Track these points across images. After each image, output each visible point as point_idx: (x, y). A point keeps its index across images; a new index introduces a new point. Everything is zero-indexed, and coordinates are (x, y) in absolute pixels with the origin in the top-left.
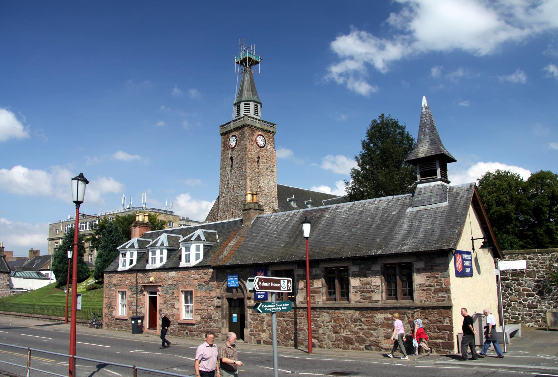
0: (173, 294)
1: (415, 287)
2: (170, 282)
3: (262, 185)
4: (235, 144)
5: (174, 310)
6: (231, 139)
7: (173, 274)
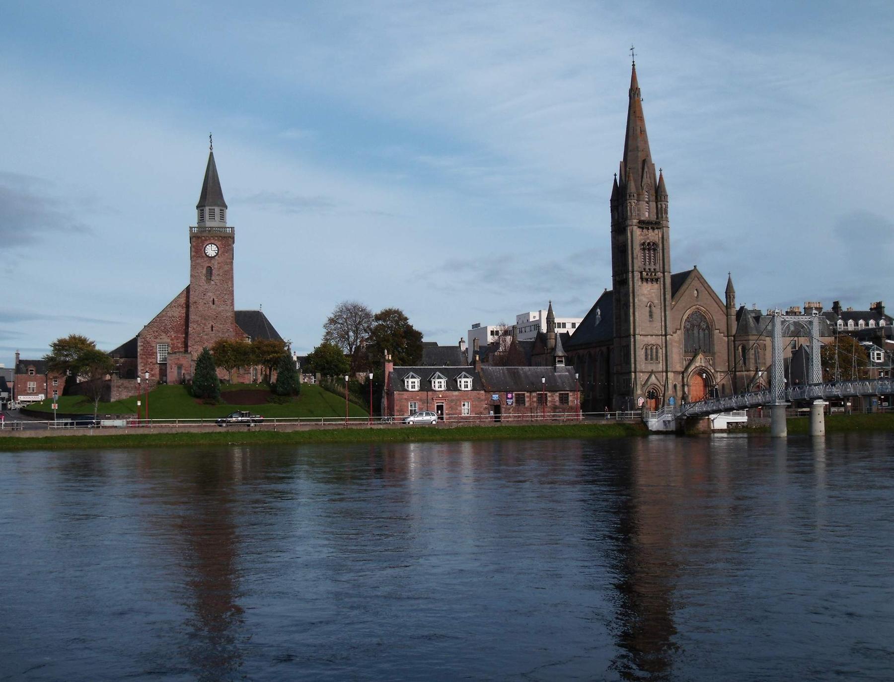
0: (456, 403)
1: (569, 401)
2: (454, 398)
4: (215, 254)
6: (208, 247)
7: (456, 393)
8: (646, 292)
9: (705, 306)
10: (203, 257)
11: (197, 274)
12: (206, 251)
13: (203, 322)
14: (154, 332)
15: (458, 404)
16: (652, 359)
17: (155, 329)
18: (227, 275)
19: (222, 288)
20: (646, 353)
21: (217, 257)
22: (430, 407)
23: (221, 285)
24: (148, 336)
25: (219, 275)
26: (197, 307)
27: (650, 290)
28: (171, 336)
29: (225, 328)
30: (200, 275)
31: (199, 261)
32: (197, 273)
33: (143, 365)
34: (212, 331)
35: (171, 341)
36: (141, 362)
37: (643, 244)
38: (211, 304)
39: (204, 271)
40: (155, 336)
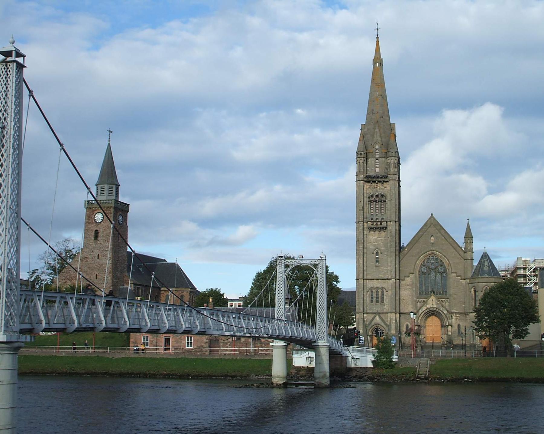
3: (120, 255)
5: (181, 344)
6: (96, 215)
8: (372, 240)
9: (440, 251)
10: (93, 223)
11: (88, 236)
12: (95, 219)
13: (91, 272)
15: (182, 338)
16: (377, 301)
20: (372, 295)
22: (159, 340)
26: (87, 261)
27: (377, 238)
30: (90, 236)
31: (91, 226)
34: (96, 279)
37: (372, 196)
38: (96, 258)
39: (93, 234)
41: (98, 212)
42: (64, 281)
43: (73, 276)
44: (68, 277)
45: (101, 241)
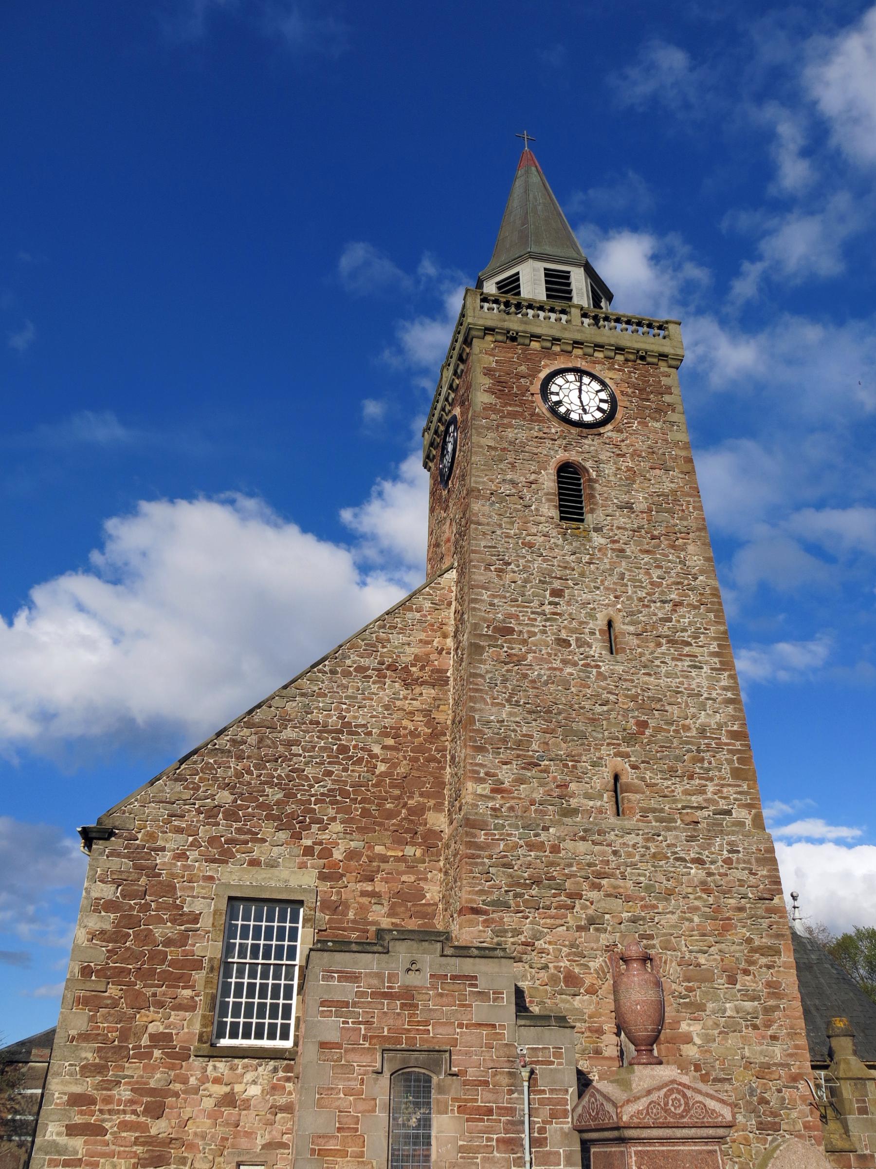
4: (599, 415)
6: (559, 381)
10: (535, 417)
14: (211, 814)
17: (225, 797)
18: (671, 512)
19: (655, 574)
21: (609, 427)
23: (647, 558)
24: (172, 842)
25: (629, 506)
26: (519, 661)
28: (326, 853)
29: (695, 800)
32: (513, 483)
33: (89, 1055)
35: (325, 886)
36: (84, 1037)
38: (597, 649)
39: (548, 481)
40: (212, 841)
41: (570, 365)
42: (224, 828)
43: (316, 789)
44: (274, 795)
45: (624, 536)
